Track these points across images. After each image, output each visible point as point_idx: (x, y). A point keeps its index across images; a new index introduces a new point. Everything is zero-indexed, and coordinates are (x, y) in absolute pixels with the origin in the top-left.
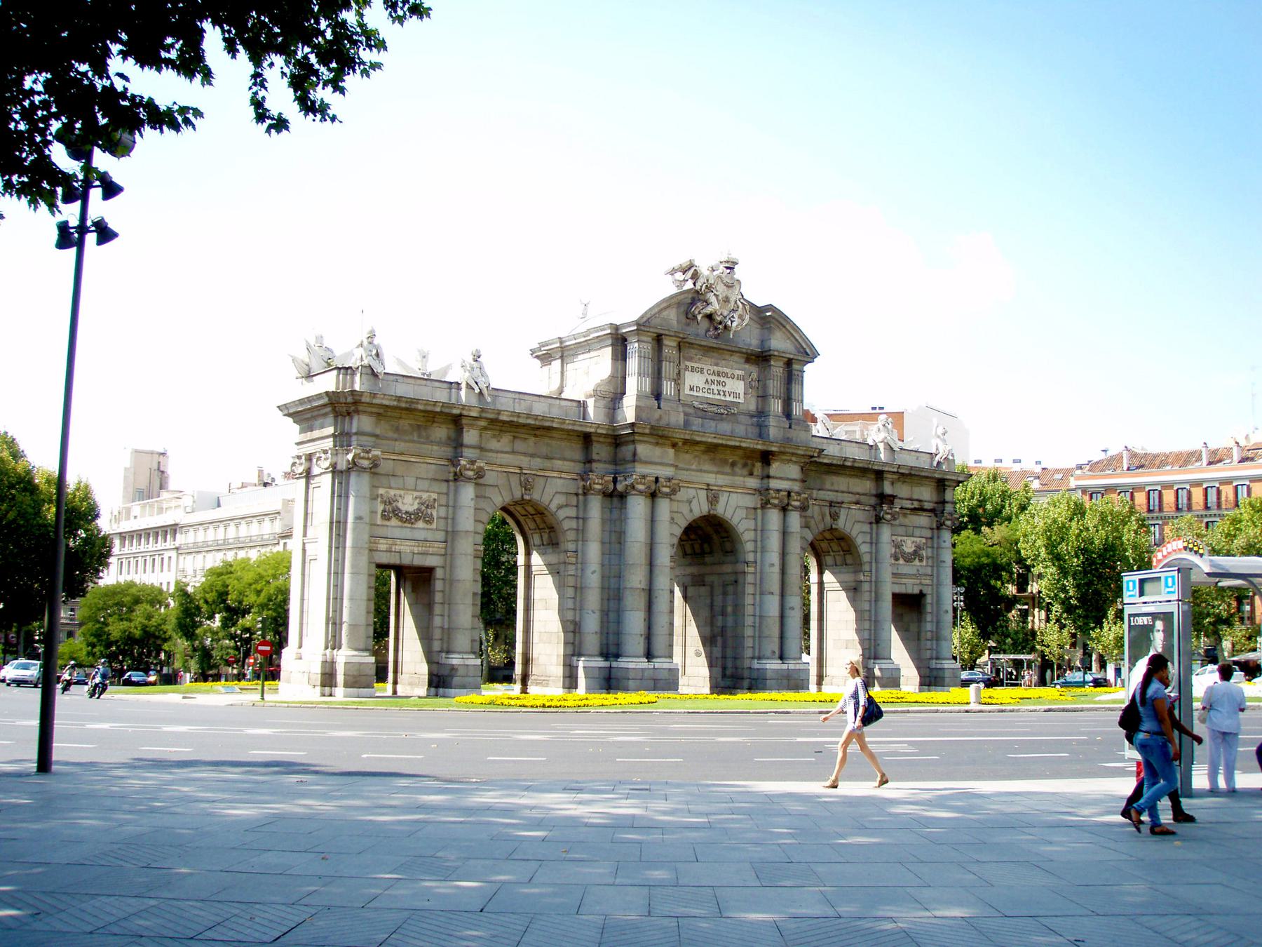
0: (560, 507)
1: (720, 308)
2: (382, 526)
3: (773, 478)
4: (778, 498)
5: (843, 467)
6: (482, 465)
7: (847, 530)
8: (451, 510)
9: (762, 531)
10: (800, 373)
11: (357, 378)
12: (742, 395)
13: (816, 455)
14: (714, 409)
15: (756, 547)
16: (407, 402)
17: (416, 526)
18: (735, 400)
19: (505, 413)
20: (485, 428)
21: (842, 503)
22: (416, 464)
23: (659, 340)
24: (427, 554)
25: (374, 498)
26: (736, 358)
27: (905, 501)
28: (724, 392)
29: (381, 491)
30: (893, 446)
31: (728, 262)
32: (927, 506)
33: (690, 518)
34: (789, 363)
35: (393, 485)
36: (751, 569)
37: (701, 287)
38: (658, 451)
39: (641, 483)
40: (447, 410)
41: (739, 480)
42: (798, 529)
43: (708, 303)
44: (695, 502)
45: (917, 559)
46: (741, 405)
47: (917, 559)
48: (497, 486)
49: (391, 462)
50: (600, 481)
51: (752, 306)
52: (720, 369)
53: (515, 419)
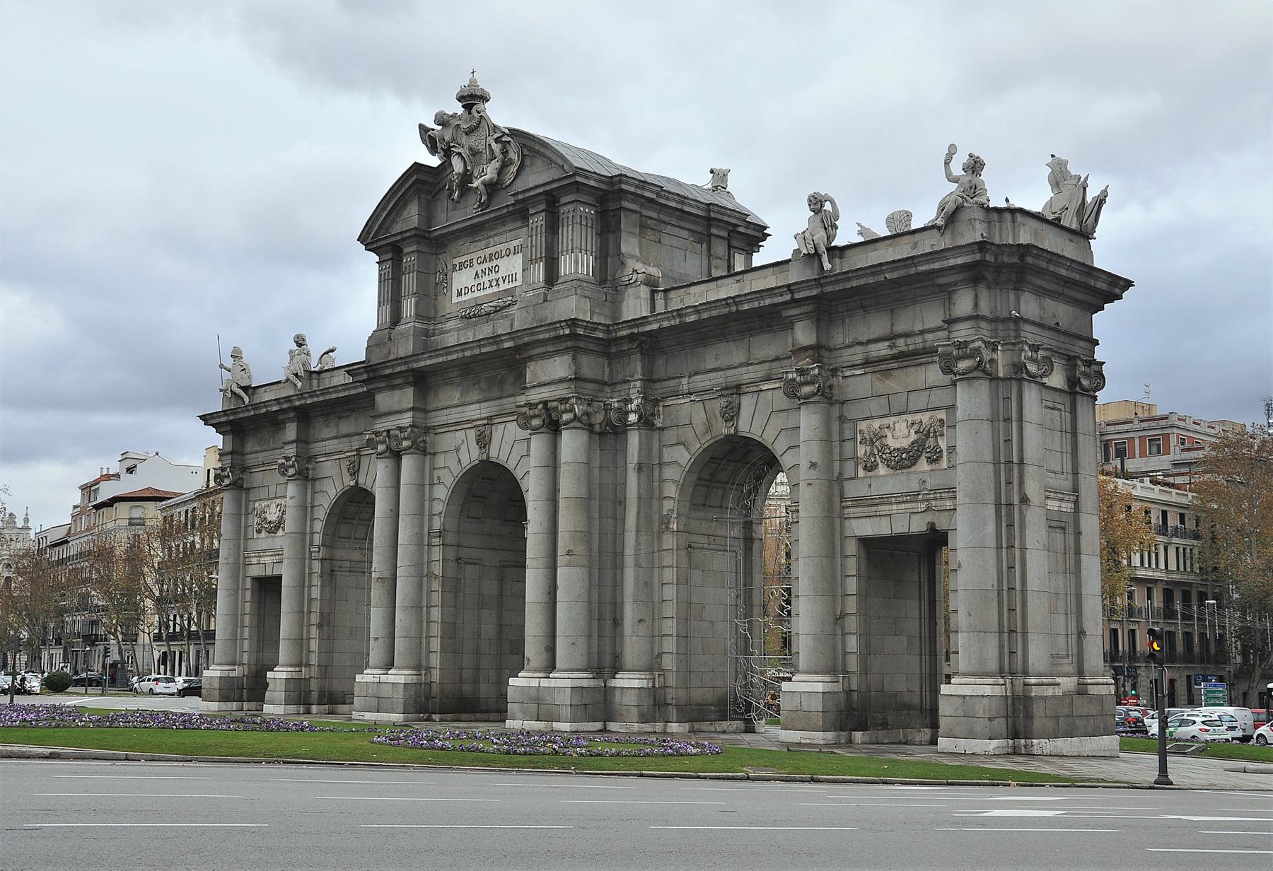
12: (519, 277)
17: (277, 534)
18: (511, 285)
27: (873, 347)
33: (457, 471)
44: (464, 447)
52: (492, 250)
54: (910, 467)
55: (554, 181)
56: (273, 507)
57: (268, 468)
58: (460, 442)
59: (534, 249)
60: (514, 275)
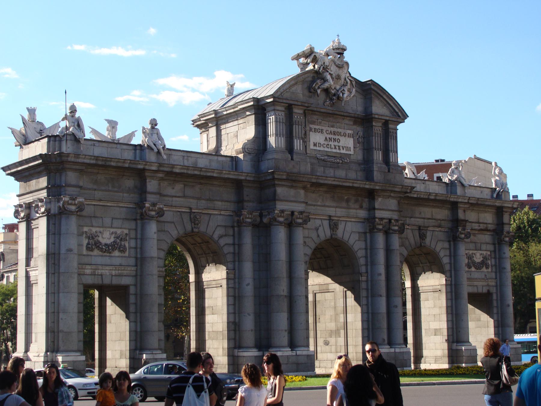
0: (221, 237)
1: (334, 83)
2: (88, 255)
3: (378, 209)
4: (382, 224)
5: (428, 200)
6: (161, 206)
7: (433, 246)
8: (139, 241)
9: (371, 250)
10: (394, 131)
11: (64, 143)
13: (408, 191)
14: (332, 159)
15: (367, 261)
16: (103, 160)
17: (113, 255)
18: (347, 152)
19: (178, 167)
20: (162, 179)
21: (428, 227)
22: (112, 208)
23: (289, 108)
24: (122, 276)
25: (80, 234)
26: (346, 121)
27: (473, 224)
28: (339, 147)
29: (86, 229)
30: (464, 183)
31: (338, 49)
32: (491, 227)
33: (317, 241)
34: (386, 123)
35: (94, 224)
36: (364, 278)
37: (320, 68)
38: (292, 192)
39: (281, 216)
40: (134, 166)
41: (353, 212)
42: (398, 247)
43: (325, 80)
44: (321, 229)
45: (484, 267)
46: (352, 157)
47: (484, 267)
48: (173, 222)
49: (92, 207)
50: (250, 216)
51: (357, 81)
53: (185, 171)
54: (481, 269)
55: (387, 116)
56: (107, 234)
57: (101, 204)
58: (318, 225)
59: (377, 143)
60: (349, 148)
